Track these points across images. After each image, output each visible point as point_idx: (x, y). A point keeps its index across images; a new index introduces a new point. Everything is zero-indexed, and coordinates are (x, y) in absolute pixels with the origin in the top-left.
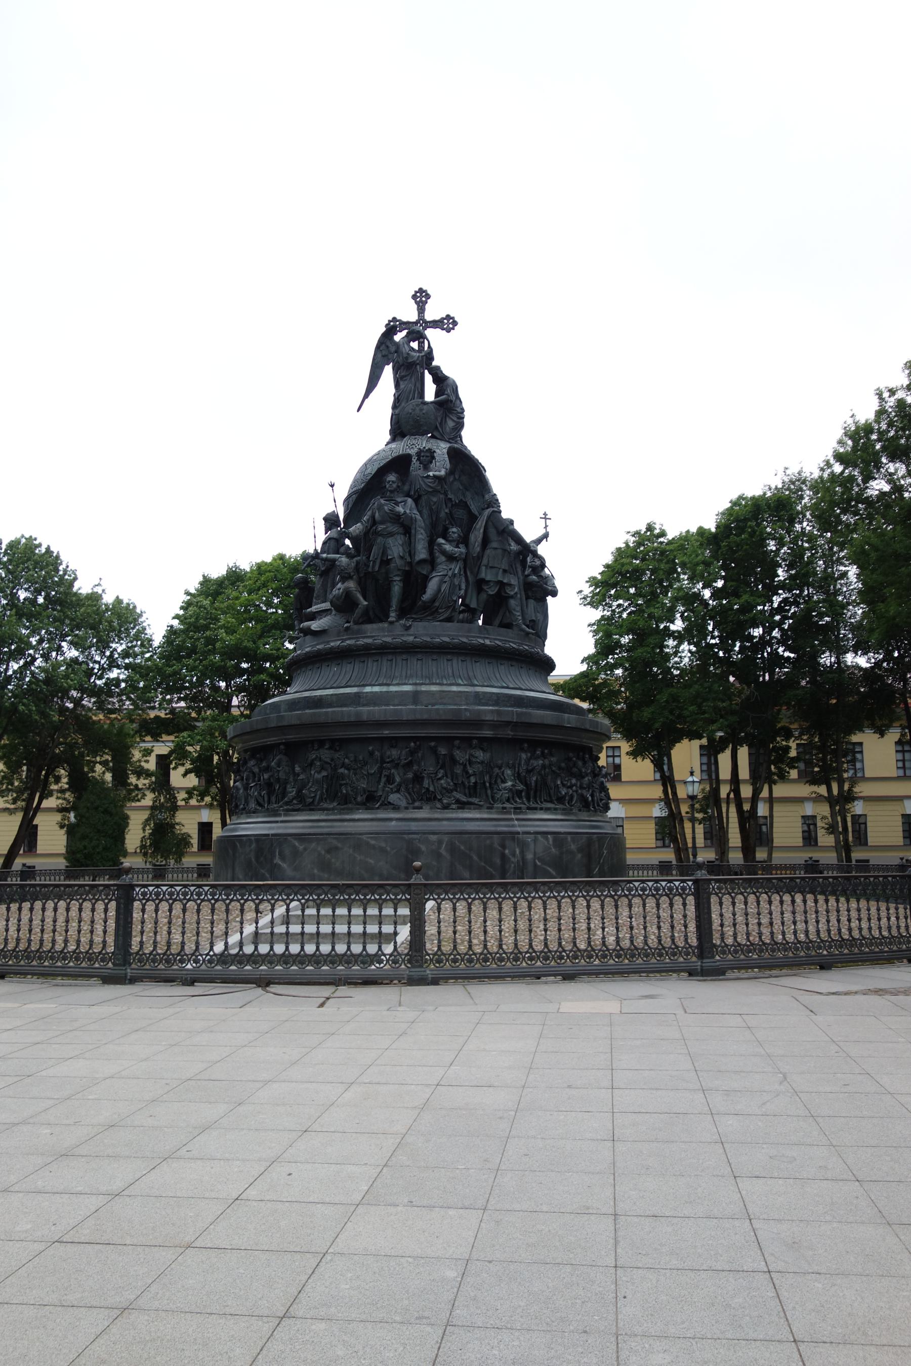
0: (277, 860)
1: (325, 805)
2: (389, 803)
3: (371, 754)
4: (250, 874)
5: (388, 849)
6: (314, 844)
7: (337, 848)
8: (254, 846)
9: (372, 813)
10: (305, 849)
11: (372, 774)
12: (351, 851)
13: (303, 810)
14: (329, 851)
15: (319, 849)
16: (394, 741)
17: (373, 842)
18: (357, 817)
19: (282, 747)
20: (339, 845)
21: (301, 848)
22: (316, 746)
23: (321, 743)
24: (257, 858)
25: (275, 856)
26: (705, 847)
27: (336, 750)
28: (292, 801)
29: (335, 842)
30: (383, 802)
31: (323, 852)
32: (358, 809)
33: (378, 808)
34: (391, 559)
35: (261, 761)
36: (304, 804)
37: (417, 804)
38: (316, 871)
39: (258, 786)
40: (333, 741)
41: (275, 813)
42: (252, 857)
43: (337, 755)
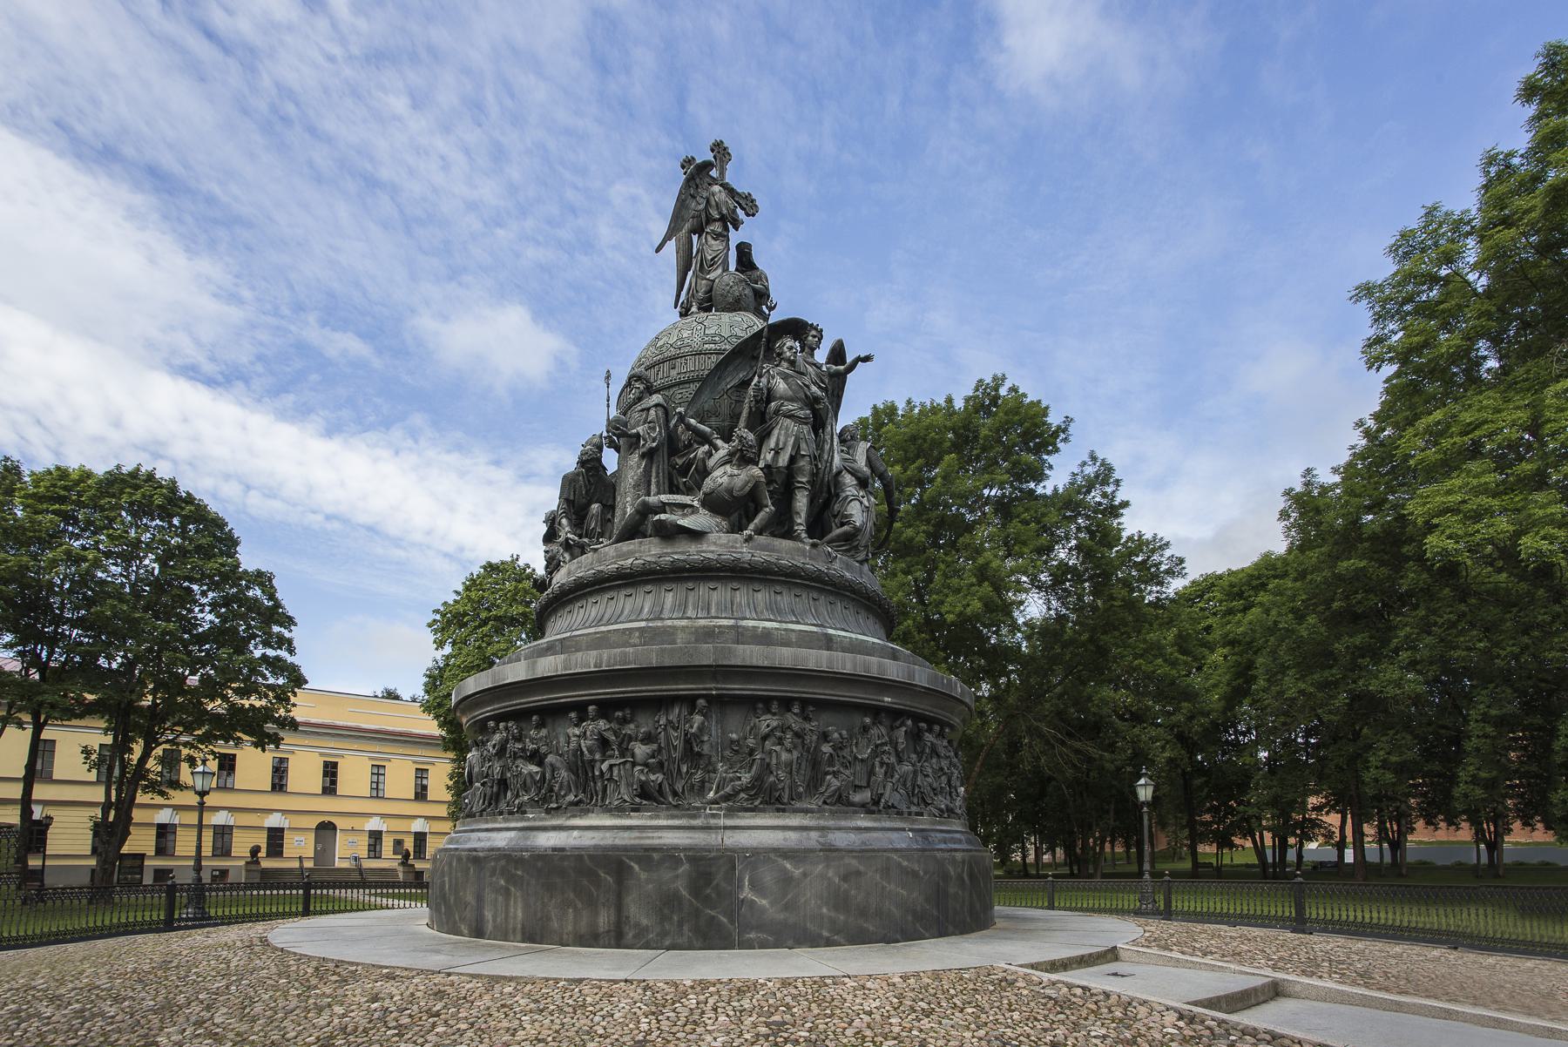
0: (747, 893)
1: (798, 805)
2: (893, 806)
3: (865, 729)
4: (675, 918)
5: (922, 873)
6: (821, 867)
7: (858, 873)
8: (685, 868)
9: (875, 820)
10: (805, 875)
11: (862, 760)
12: (878, 877)
13: (763, 811)
14: (845, 878)
15: (830, 874)
16: (876, 712)
17: (905, 863)
18: (861, 823)
19: (701, 702)
20: (862, 868)
21: (797, 872)
22: (775, 707)
23: (786, 703)
24: (696, 890)
25: (741, 887)
26: (369, 858)
27: (807, 719)
28: (738, 793)
29: (854, 862)
30: (887, 802)
31: (837, 880)
32: (855, 812)
33: (879, 811)
34: (804, 456)
35: (624, 721)
36: (766, 797)
37: (914, 809)
38: (825, 910)
39: (628, 766)
40: (804, 703)
41: (694, 813)
42: (682, 888)
43: (807, 726)
